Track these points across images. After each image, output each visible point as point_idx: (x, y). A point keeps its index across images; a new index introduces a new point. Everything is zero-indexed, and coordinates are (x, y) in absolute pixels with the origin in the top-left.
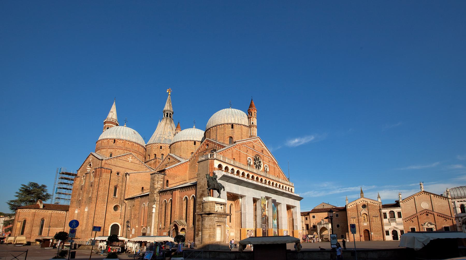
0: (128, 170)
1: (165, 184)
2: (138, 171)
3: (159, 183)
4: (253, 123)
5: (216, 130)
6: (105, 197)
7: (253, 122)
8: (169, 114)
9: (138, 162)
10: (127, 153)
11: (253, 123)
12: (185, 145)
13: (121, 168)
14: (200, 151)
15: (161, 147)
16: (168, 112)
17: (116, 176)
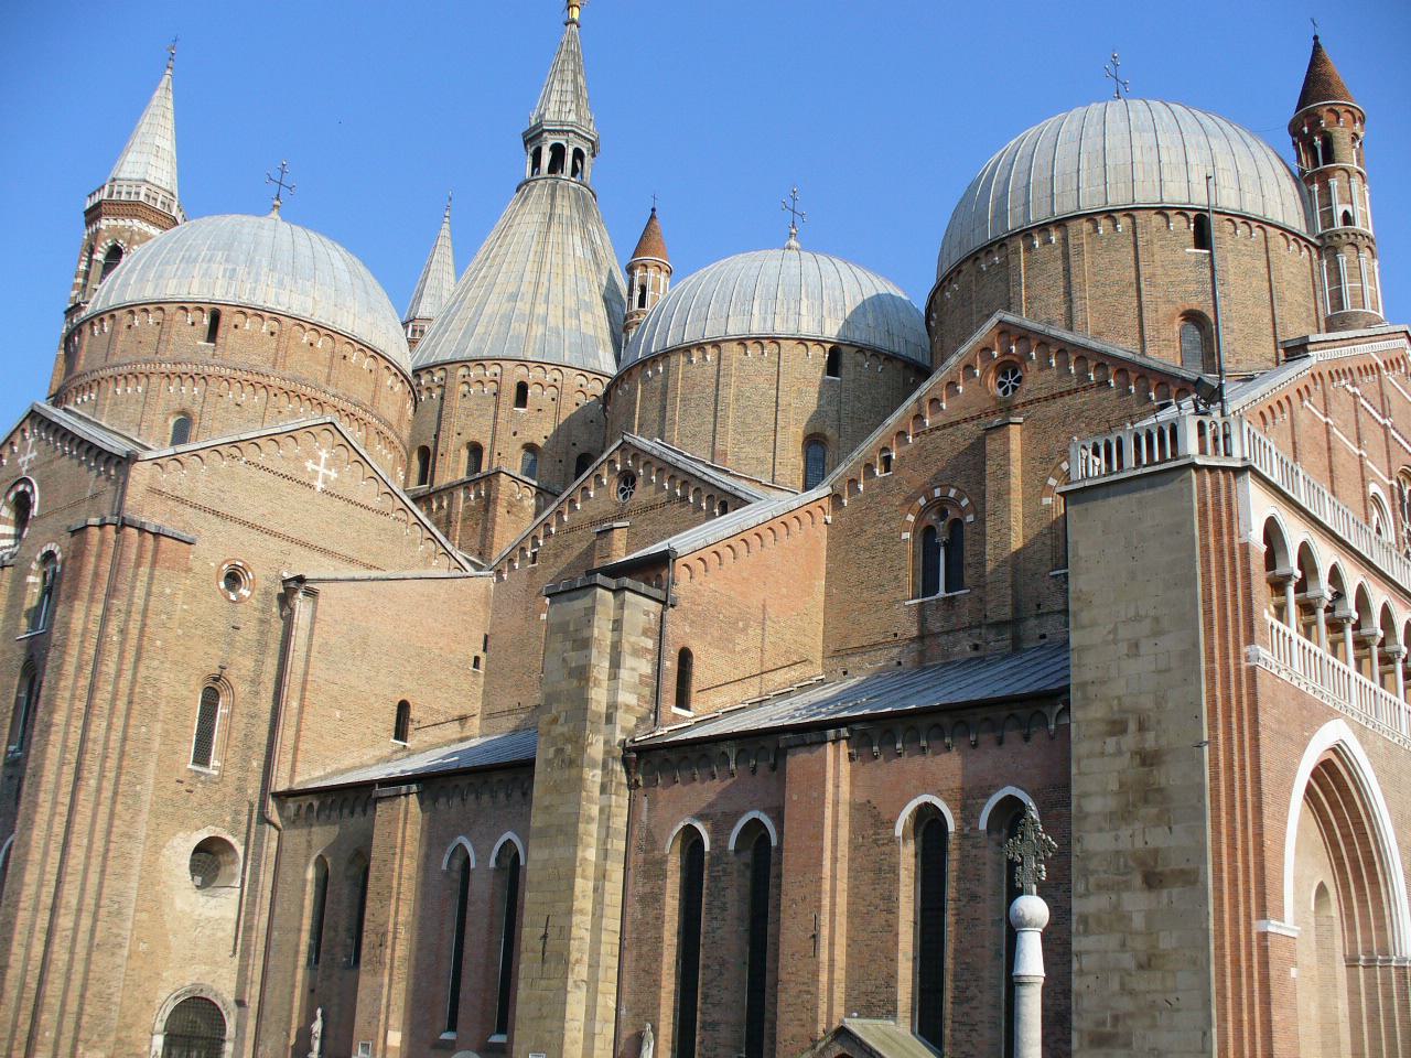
0: (304, 552)
1: (670, 682)
2: (371, 567)
3: (624, 674)
4: (1346, 214)
5: (1066, 256)
6: (136, 763)
7: (1349, 208)
9: (369, 493)
10: (294, 414)
11: (1347, 218)
12: (758, 373)
13: (254, 534)
14: (940, 419)
15: (522, 389)
17: (219, 601)
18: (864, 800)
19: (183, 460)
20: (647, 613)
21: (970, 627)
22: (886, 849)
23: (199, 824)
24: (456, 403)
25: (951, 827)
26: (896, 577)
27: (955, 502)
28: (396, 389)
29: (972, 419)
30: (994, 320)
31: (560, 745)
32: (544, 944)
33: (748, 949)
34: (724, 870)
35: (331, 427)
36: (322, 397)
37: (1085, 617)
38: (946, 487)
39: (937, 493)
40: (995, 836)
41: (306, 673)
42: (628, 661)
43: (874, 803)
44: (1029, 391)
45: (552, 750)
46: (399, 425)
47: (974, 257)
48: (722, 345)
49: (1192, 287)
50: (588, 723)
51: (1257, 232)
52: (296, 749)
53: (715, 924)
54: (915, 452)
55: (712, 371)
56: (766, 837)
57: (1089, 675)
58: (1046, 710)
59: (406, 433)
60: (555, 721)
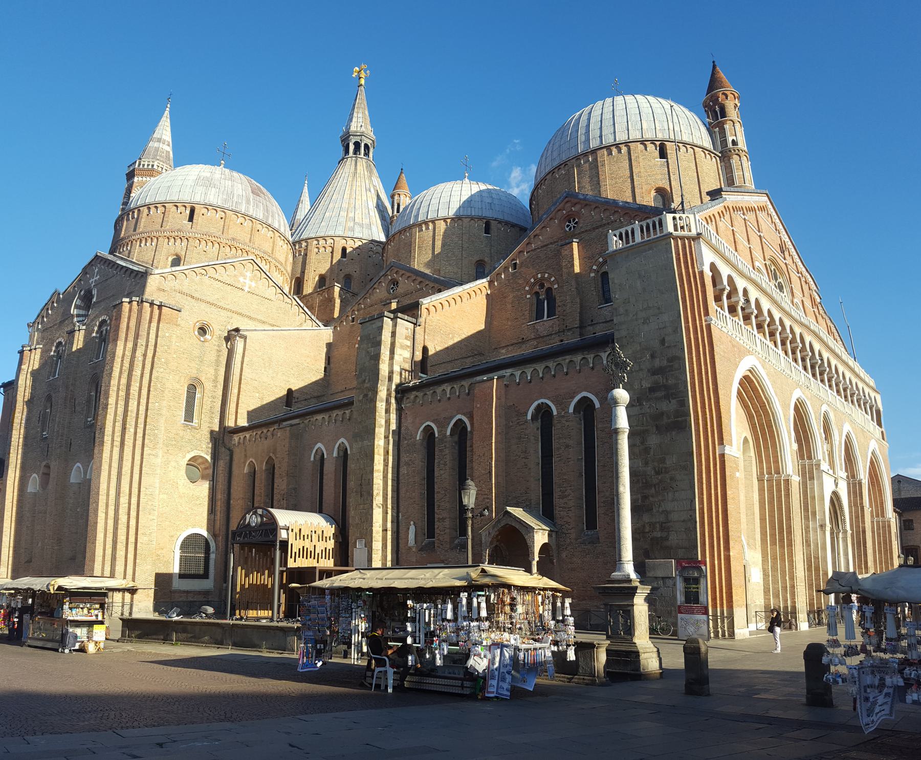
3: (396, 357)
7: (735, 138)
8: (363, 145)
9: (271, 292)
11: (734, 143)
12: (453, 234)
16: (358, 139)
19: (176, 275)
20: (407, 329)
22: (524, 427)
23: (189, 449)
24: (312, 257)
25: (555, 413)
28: (284, 247)
29: (555, 242)
31: (365, 393)
34: (445, 446)
35: (252, 262)
36: (247, 249)
38: (543, 273)
39: (539, 276)
41: (241, 375)
42: (398, 351)
44: (582, 227)
45: (361, 396)
46: (286, 263)
48: (436, 222)
49: (659, 177)
50: (380, 381)
51: (690, 150)
52: (237, 412)
53: (442, 472)
54: (528, 260)
55: (431, 234)
56: (465, 428)
59: (289, 269)
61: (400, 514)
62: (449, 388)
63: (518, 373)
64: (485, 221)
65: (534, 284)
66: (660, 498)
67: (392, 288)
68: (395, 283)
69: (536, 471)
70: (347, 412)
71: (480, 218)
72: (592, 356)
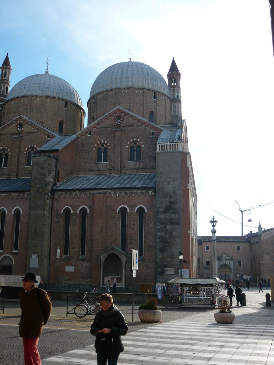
4: (177, 95)
18: (110, 205)
21: (109, 170)
22: (115, 215)
25: (128, 211)
26: (92, 157)
27: (106, 144)
29: (111, 127)
30: (117, 107)
32: (36, 231)
33: (81, 233)
37: (159, 176)
38: (104, 140)
39: (102, 141)
40: (137, 214)
43: (112, 206)
44: (124, 124)
45: (36, 190)
47: (108, 91)
53: (74, 227)
57: (160, 187)
58: (149, 192)
60: (36, 184)
61: (51, 244)
62: (79, 193)
63: (113, 193)
64: (65, 101)
65: (99, 144)
66: (171, 247)
67: (19, 128)
68: (21, 125)
69: (120, 232)
70: (21, 195)
71: (63, 100)
72: (146, 191)
